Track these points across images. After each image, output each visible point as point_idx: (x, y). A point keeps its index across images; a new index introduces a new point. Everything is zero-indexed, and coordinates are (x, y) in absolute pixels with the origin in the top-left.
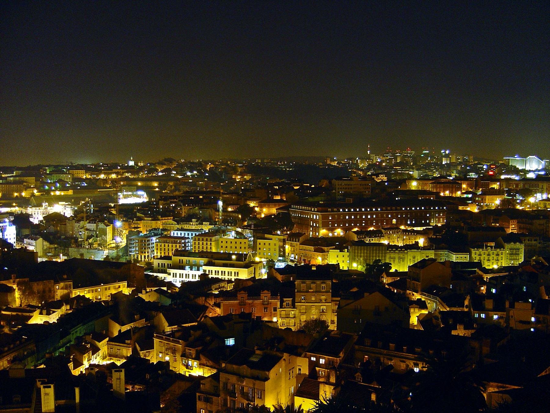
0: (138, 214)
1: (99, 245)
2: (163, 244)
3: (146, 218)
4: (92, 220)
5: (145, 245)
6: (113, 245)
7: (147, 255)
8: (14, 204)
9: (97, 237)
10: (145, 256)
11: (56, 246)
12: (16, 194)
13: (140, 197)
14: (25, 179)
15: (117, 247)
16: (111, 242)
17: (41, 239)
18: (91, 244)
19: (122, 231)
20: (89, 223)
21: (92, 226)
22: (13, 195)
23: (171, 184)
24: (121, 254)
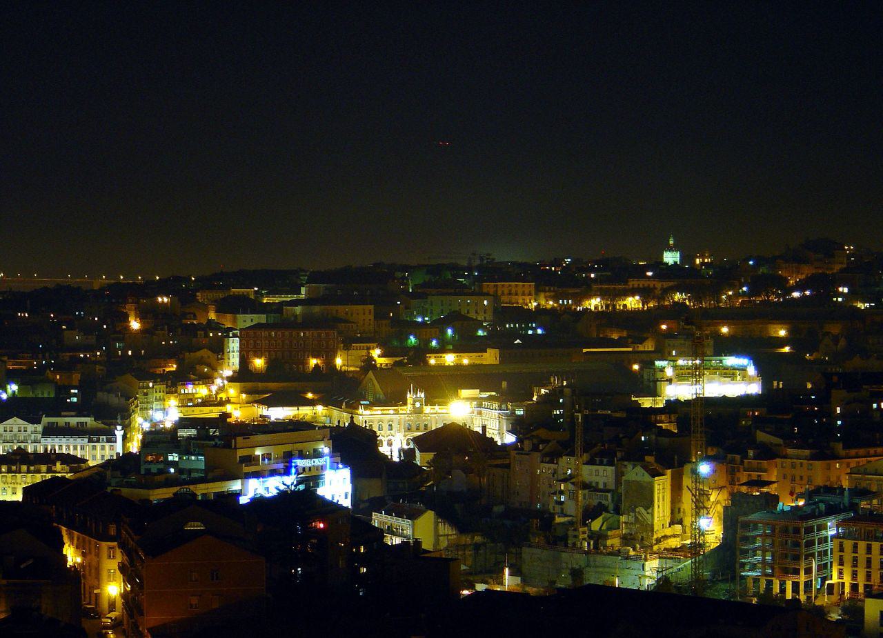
0: (761, 436)
1: (627, 540)
2: (862, 545)
3: (790, 451)
4: (602, 454)
5: (797, 544)
6: (674, 543)
7: (802, 578)
8: (310, 396)
9: (618, 511)
10: (796, 586)
11: (478, 539)
12: (313, 362)
13: (733, 376)
14: (343, 310)
15: (695, 549)
16: (669, 532)
17: (429, 516)
18: (598, 537)
19: (708, 495)
20: (591, 462)
21: (602, 475)
22: (305, 363)
23: (835, 329)
24: (707, 574)
